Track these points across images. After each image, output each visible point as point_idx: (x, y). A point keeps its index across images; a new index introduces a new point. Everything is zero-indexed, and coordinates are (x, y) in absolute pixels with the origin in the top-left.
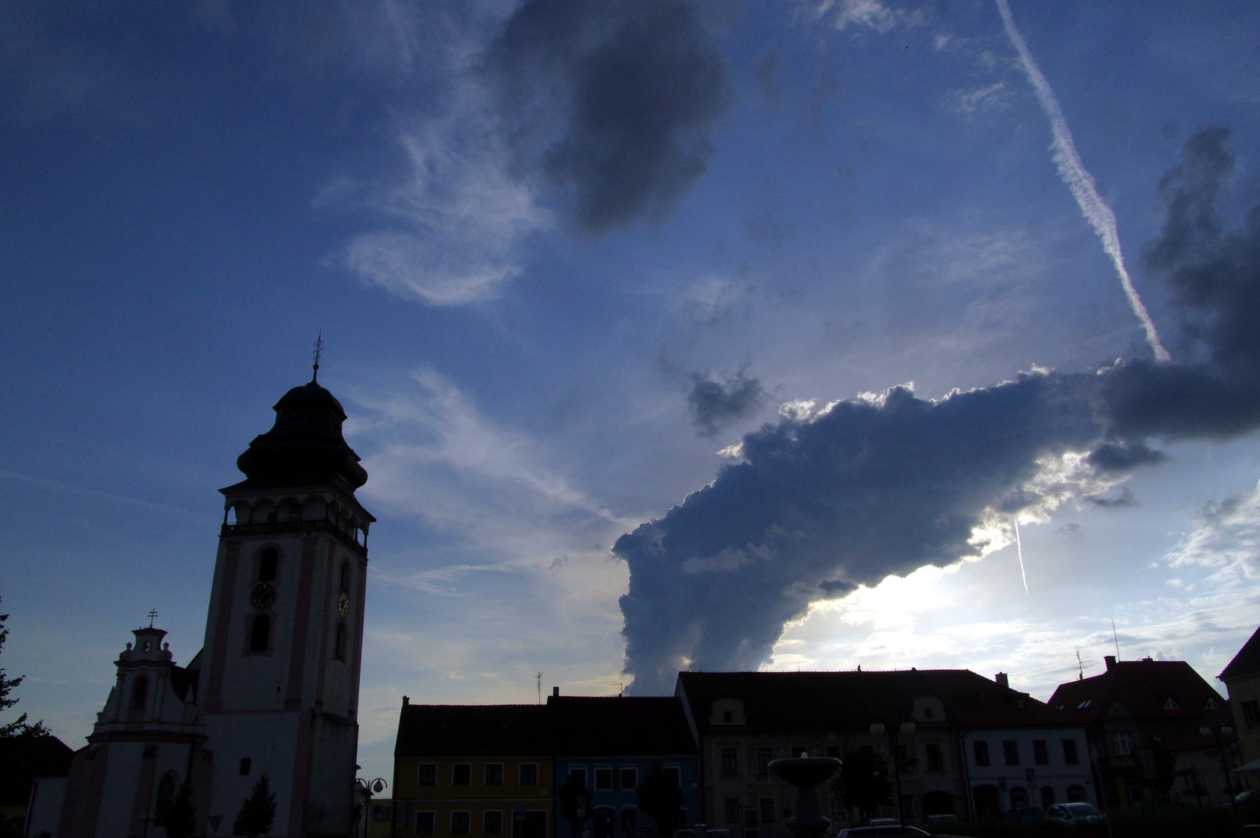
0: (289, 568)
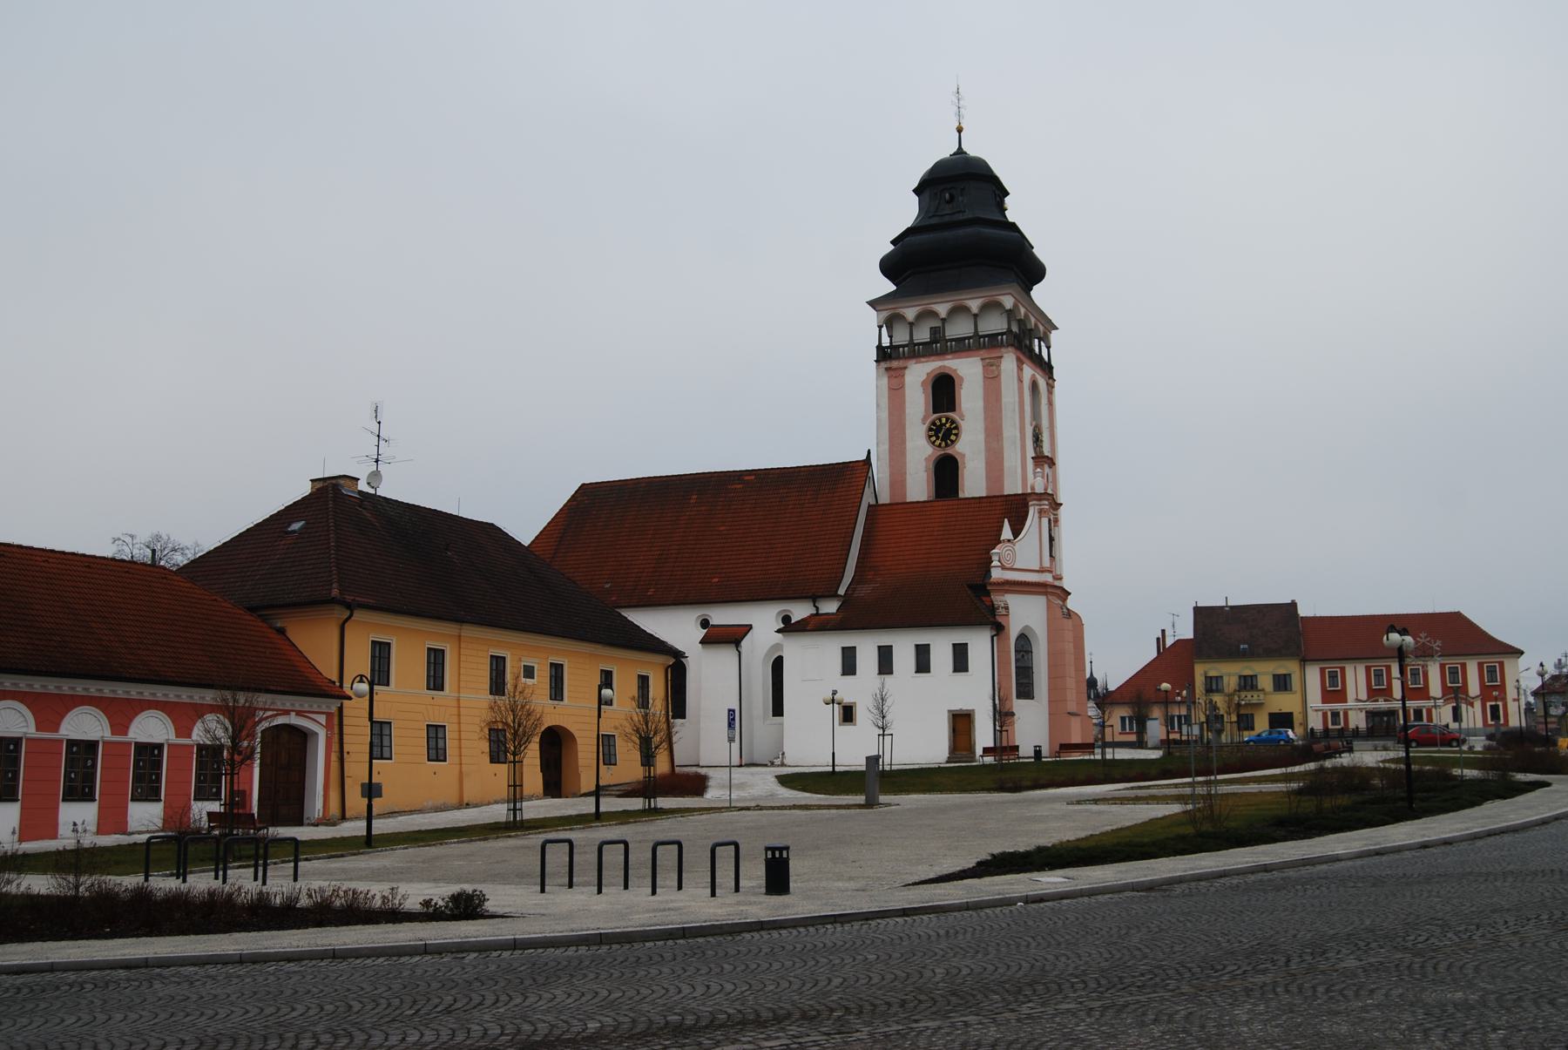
0: (970, 398)
